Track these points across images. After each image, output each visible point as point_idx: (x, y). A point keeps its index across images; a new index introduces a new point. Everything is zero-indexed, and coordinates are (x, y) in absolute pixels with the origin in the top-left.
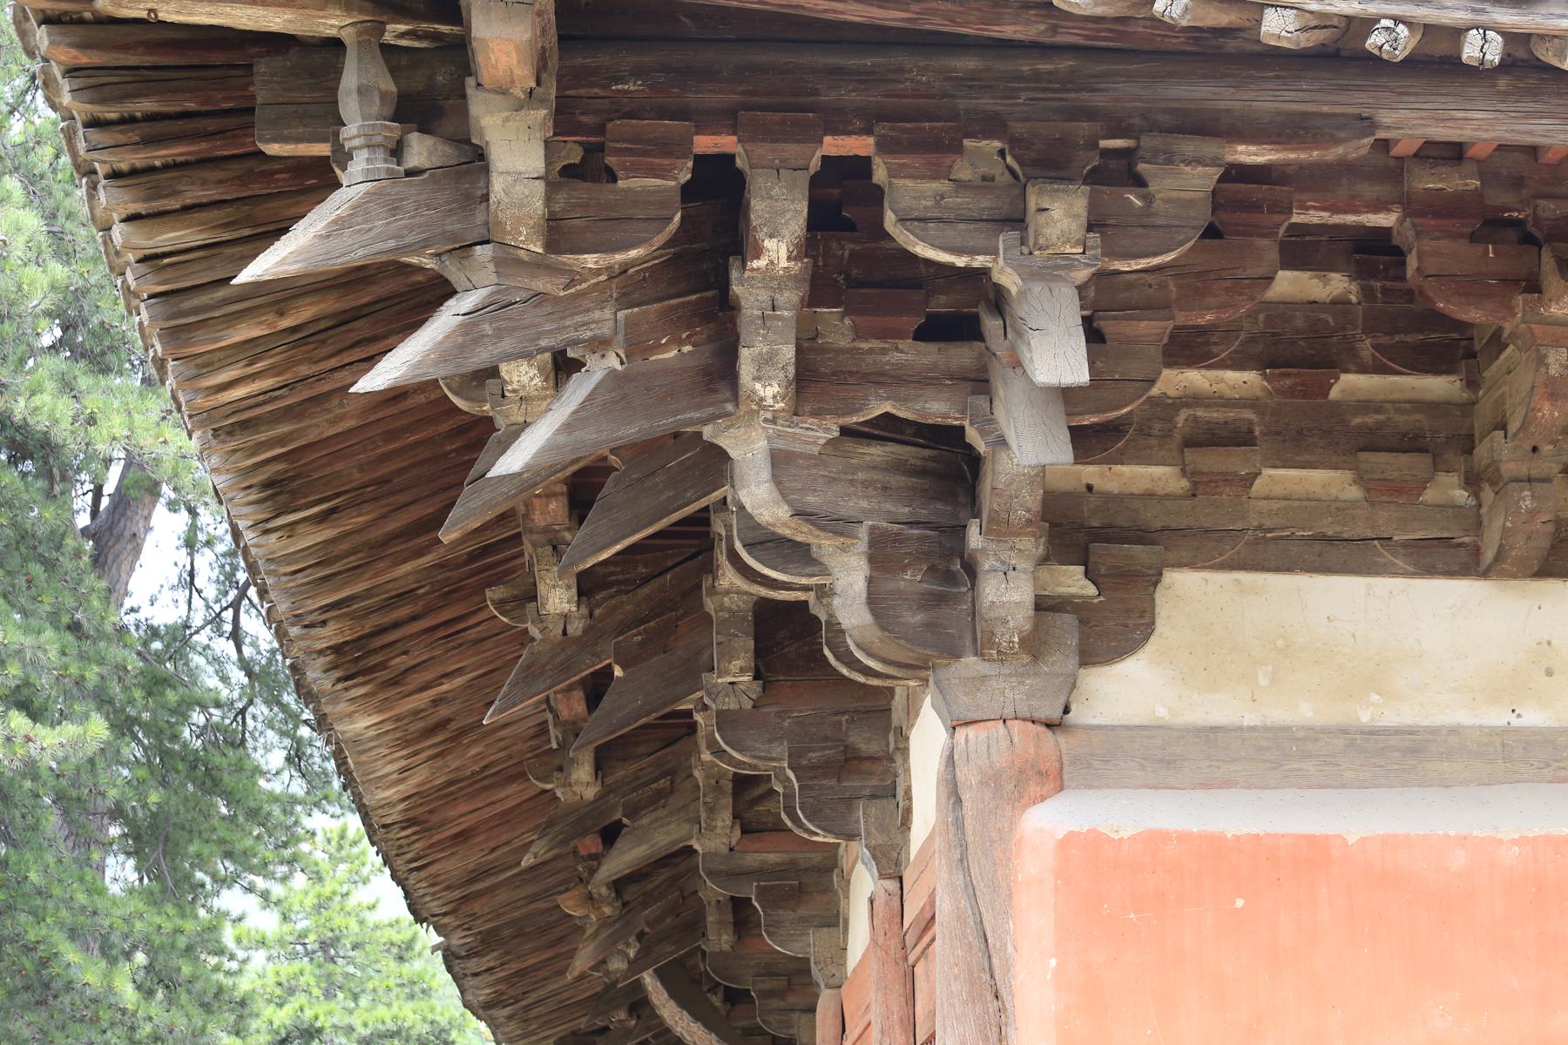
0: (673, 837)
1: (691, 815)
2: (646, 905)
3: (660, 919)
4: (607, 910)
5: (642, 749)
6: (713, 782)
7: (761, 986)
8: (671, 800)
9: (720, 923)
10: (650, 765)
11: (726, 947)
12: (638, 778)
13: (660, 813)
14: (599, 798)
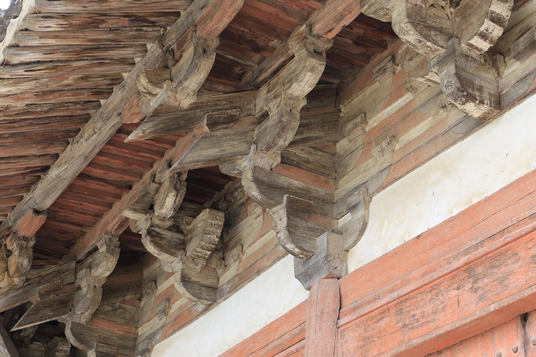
0: (236, 150)
1: (248, 139)
2: (39, 283)
3: (48, 293)
4: (16, 280)
5: (221, 88)
6: (289, 109)
7: (100, 349)
8: (236, 127)
9: (93, 300)
10: (225, 100)
11: (83, 321)
12: (216, 105)
13: (228, 131)
14: (194, 107)
